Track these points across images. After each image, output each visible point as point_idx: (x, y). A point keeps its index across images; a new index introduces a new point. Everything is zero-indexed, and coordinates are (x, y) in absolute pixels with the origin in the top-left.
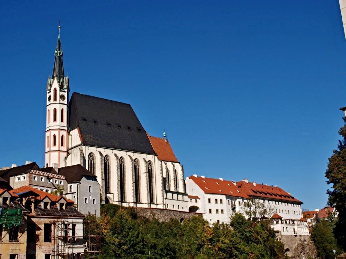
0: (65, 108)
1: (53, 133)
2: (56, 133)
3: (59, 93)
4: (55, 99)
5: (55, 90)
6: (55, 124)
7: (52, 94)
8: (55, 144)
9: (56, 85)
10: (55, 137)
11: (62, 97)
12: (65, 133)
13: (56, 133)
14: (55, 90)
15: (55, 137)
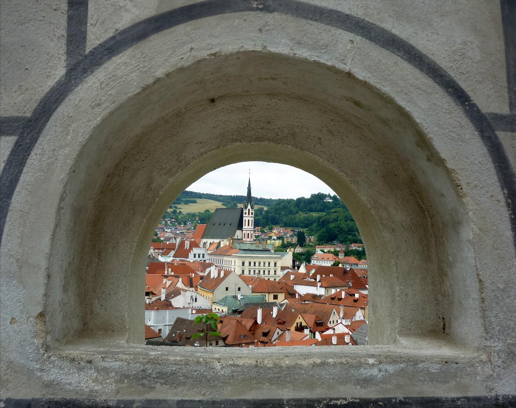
0: (253, 219)
1: (248, 232)
2: (249, 232)
3: (251, 212)
4: (249, 214)
5: (249, 210)
6: (248, 227)
7: (247, 211)
8: (248, 238)
9: (249, 207)
10: (248, 234)
11: (252, 214)
12: (252, 232)
13: (249, 232)
14: (249, 210)
15: (248, 234)
